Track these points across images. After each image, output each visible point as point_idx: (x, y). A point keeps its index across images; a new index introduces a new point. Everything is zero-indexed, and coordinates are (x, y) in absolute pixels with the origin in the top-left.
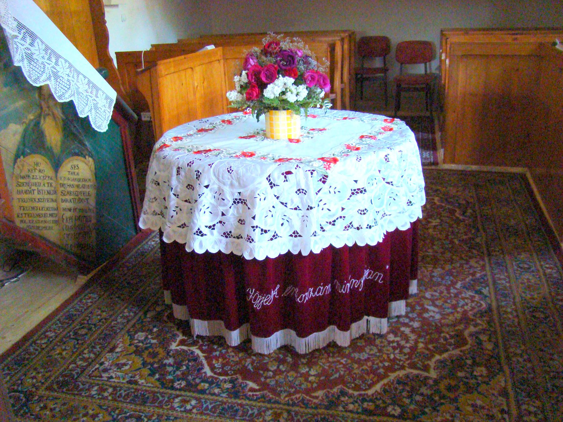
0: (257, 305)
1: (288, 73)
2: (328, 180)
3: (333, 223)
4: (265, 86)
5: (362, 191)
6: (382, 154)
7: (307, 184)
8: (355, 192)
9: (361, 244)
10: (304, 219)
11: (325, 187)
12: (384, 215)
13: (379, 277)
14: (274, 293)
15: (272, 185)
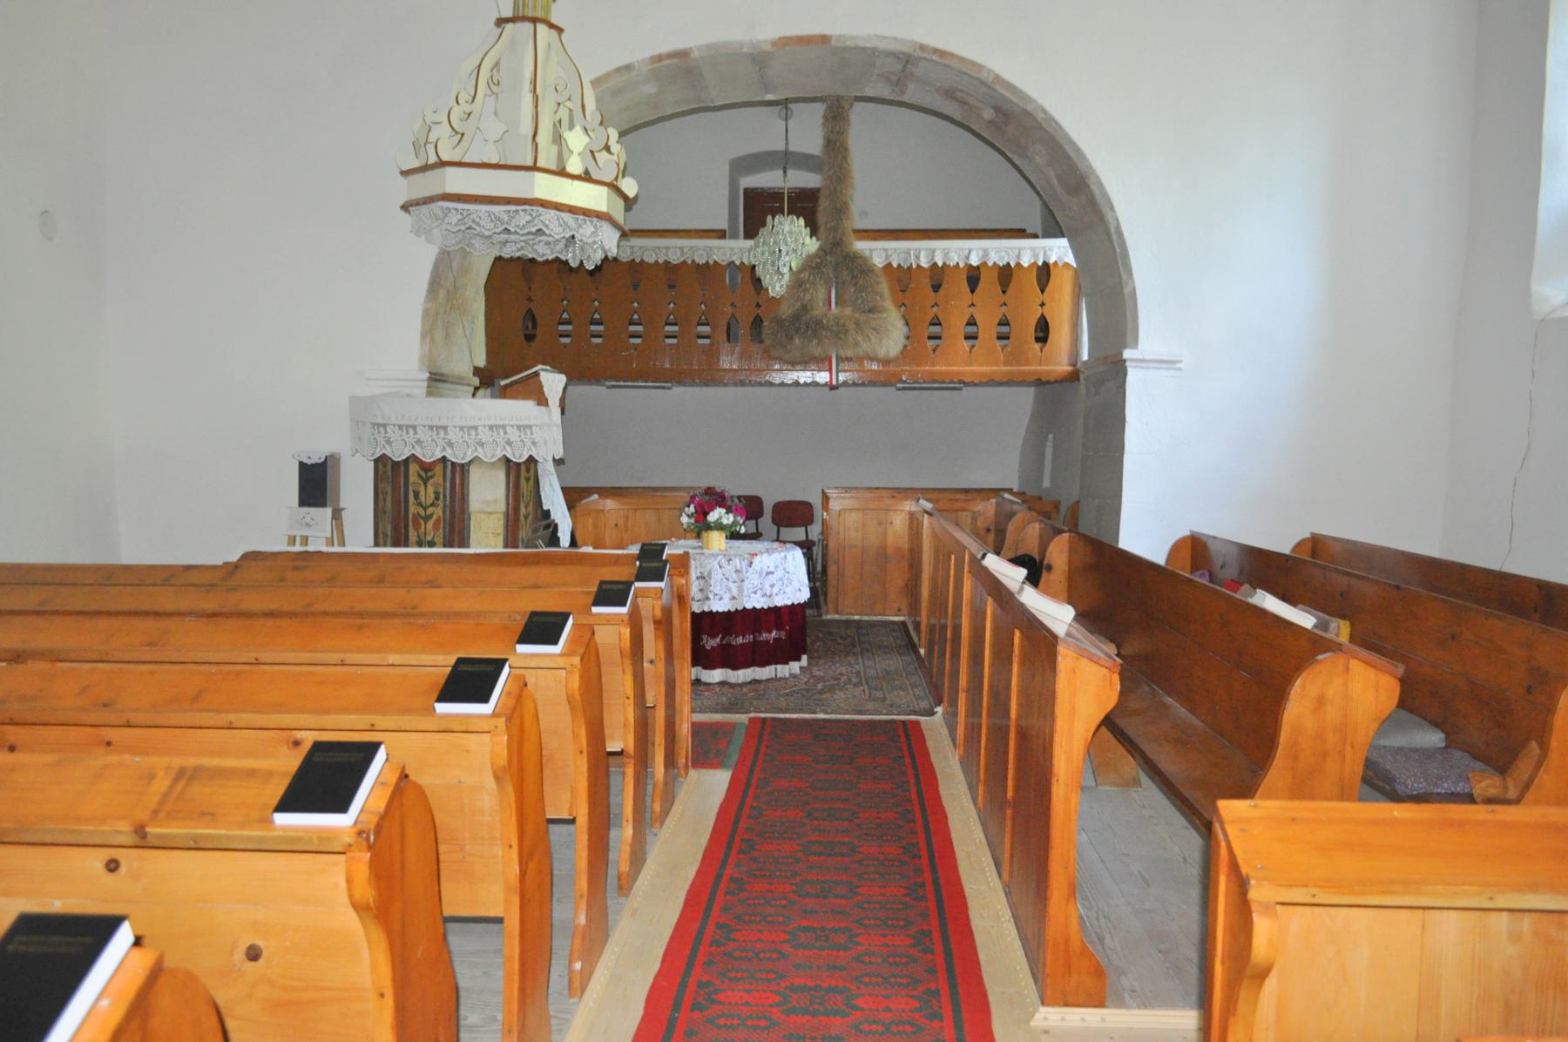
0: (708, 648)
1: (721, 506)
2: (753, 565)
3: (755, 593)
4: (708, 513)
5: (772, 573)
6: (783, 554)
7: (741, 567)
8: (768, 573)
9: (772, 606)
10: (741, 589)
11: (751, 570)
12: (784, 592)
13: (783, 635)
14: (718, 640)
15: (720, 567)
